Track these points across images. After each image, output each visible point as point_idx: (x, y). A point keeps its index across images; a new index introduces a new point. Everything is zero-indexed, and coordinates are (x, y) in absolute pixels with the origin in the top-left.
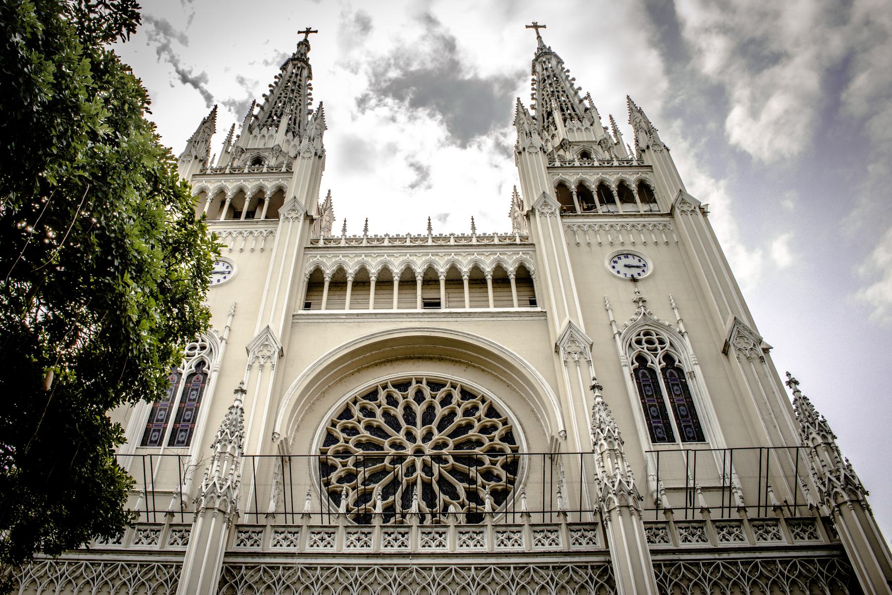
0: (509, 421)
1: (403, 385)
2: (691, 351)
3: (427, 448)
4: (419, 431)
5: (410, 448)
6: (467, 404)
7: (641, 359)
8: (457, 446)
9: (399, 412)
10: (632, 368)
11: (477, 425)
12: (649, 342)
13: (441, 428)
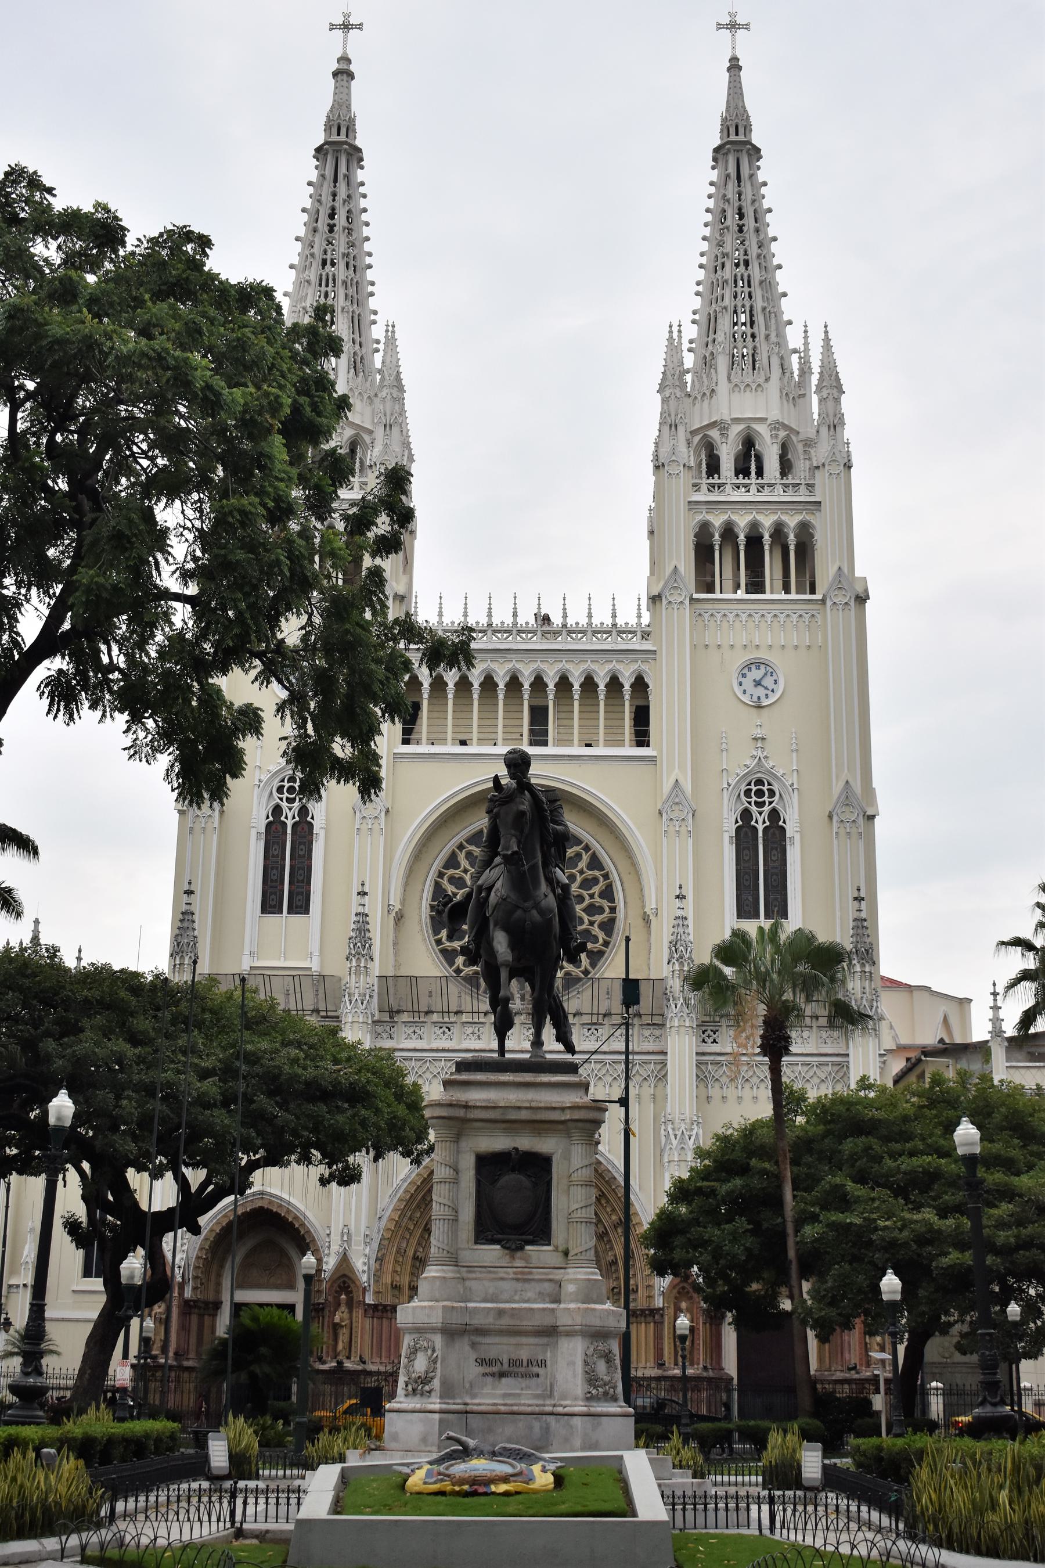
0: (611, 876)
2: (796, 816)
7: (746, 814)
10: (734, 827)
11: (579, 879)
12: (760, 793)
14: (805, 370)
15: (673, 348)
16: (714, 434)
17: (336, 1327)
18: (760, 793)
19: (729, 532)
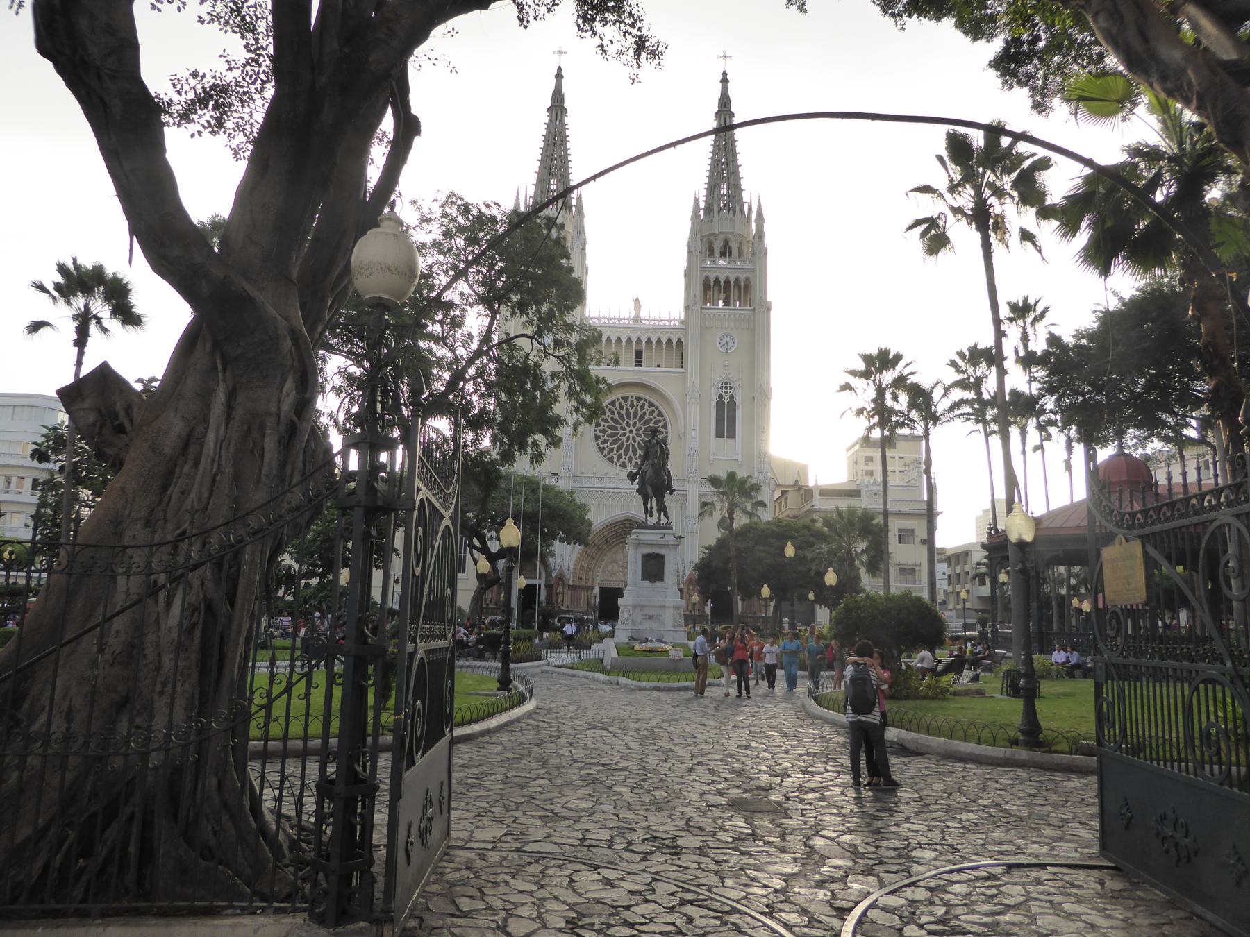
1: (625, 399)
3: (634, 429)
4: (631, 422)
5: (628, 429)
6: (650, 409)
7: (721, 396)
8: (645, 430)
9: (624, 412)
12: (726, 388)
13: (640, 421)
14: (750, 210)
15: (697, 202)
16: (712, 238)
17: (558, 594)
18: (726, 388)
19: (717, 281)
